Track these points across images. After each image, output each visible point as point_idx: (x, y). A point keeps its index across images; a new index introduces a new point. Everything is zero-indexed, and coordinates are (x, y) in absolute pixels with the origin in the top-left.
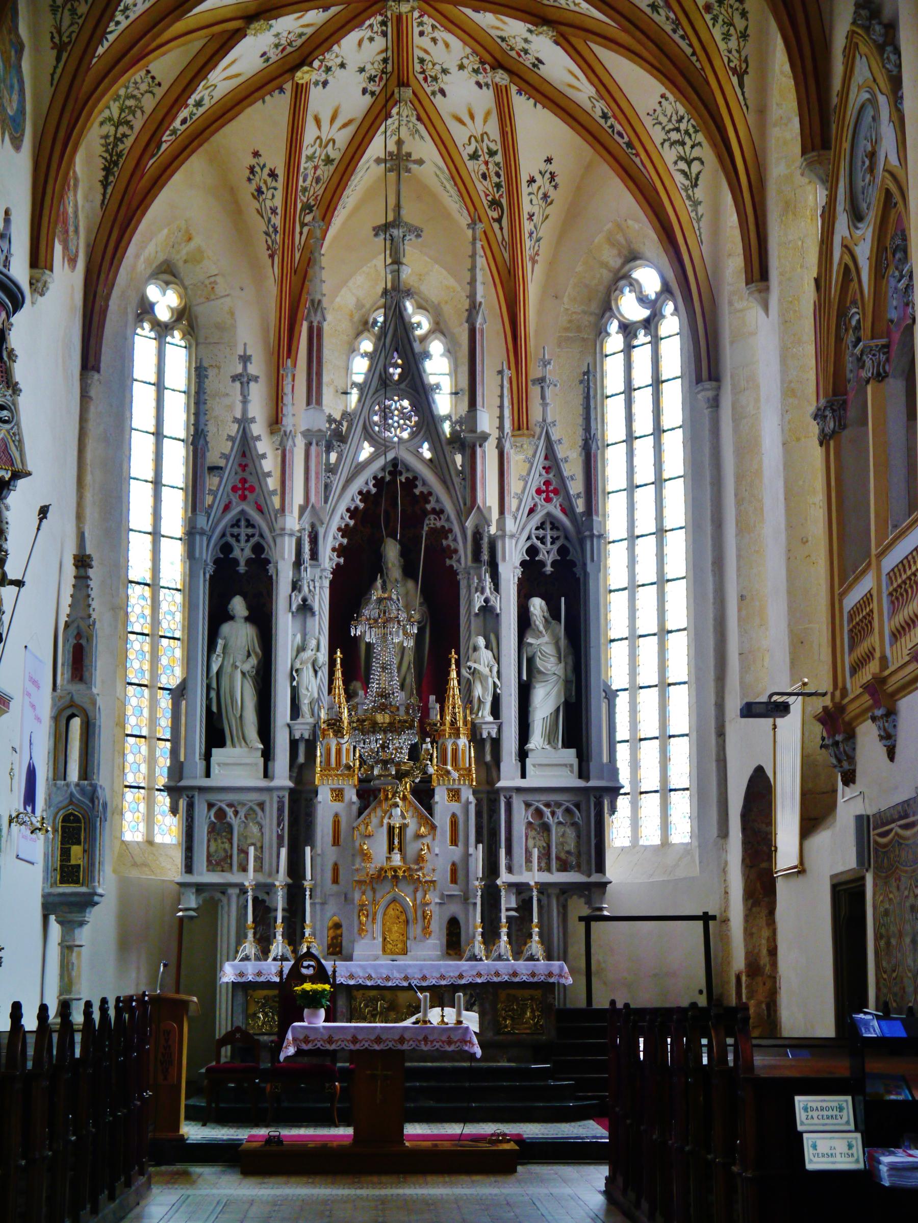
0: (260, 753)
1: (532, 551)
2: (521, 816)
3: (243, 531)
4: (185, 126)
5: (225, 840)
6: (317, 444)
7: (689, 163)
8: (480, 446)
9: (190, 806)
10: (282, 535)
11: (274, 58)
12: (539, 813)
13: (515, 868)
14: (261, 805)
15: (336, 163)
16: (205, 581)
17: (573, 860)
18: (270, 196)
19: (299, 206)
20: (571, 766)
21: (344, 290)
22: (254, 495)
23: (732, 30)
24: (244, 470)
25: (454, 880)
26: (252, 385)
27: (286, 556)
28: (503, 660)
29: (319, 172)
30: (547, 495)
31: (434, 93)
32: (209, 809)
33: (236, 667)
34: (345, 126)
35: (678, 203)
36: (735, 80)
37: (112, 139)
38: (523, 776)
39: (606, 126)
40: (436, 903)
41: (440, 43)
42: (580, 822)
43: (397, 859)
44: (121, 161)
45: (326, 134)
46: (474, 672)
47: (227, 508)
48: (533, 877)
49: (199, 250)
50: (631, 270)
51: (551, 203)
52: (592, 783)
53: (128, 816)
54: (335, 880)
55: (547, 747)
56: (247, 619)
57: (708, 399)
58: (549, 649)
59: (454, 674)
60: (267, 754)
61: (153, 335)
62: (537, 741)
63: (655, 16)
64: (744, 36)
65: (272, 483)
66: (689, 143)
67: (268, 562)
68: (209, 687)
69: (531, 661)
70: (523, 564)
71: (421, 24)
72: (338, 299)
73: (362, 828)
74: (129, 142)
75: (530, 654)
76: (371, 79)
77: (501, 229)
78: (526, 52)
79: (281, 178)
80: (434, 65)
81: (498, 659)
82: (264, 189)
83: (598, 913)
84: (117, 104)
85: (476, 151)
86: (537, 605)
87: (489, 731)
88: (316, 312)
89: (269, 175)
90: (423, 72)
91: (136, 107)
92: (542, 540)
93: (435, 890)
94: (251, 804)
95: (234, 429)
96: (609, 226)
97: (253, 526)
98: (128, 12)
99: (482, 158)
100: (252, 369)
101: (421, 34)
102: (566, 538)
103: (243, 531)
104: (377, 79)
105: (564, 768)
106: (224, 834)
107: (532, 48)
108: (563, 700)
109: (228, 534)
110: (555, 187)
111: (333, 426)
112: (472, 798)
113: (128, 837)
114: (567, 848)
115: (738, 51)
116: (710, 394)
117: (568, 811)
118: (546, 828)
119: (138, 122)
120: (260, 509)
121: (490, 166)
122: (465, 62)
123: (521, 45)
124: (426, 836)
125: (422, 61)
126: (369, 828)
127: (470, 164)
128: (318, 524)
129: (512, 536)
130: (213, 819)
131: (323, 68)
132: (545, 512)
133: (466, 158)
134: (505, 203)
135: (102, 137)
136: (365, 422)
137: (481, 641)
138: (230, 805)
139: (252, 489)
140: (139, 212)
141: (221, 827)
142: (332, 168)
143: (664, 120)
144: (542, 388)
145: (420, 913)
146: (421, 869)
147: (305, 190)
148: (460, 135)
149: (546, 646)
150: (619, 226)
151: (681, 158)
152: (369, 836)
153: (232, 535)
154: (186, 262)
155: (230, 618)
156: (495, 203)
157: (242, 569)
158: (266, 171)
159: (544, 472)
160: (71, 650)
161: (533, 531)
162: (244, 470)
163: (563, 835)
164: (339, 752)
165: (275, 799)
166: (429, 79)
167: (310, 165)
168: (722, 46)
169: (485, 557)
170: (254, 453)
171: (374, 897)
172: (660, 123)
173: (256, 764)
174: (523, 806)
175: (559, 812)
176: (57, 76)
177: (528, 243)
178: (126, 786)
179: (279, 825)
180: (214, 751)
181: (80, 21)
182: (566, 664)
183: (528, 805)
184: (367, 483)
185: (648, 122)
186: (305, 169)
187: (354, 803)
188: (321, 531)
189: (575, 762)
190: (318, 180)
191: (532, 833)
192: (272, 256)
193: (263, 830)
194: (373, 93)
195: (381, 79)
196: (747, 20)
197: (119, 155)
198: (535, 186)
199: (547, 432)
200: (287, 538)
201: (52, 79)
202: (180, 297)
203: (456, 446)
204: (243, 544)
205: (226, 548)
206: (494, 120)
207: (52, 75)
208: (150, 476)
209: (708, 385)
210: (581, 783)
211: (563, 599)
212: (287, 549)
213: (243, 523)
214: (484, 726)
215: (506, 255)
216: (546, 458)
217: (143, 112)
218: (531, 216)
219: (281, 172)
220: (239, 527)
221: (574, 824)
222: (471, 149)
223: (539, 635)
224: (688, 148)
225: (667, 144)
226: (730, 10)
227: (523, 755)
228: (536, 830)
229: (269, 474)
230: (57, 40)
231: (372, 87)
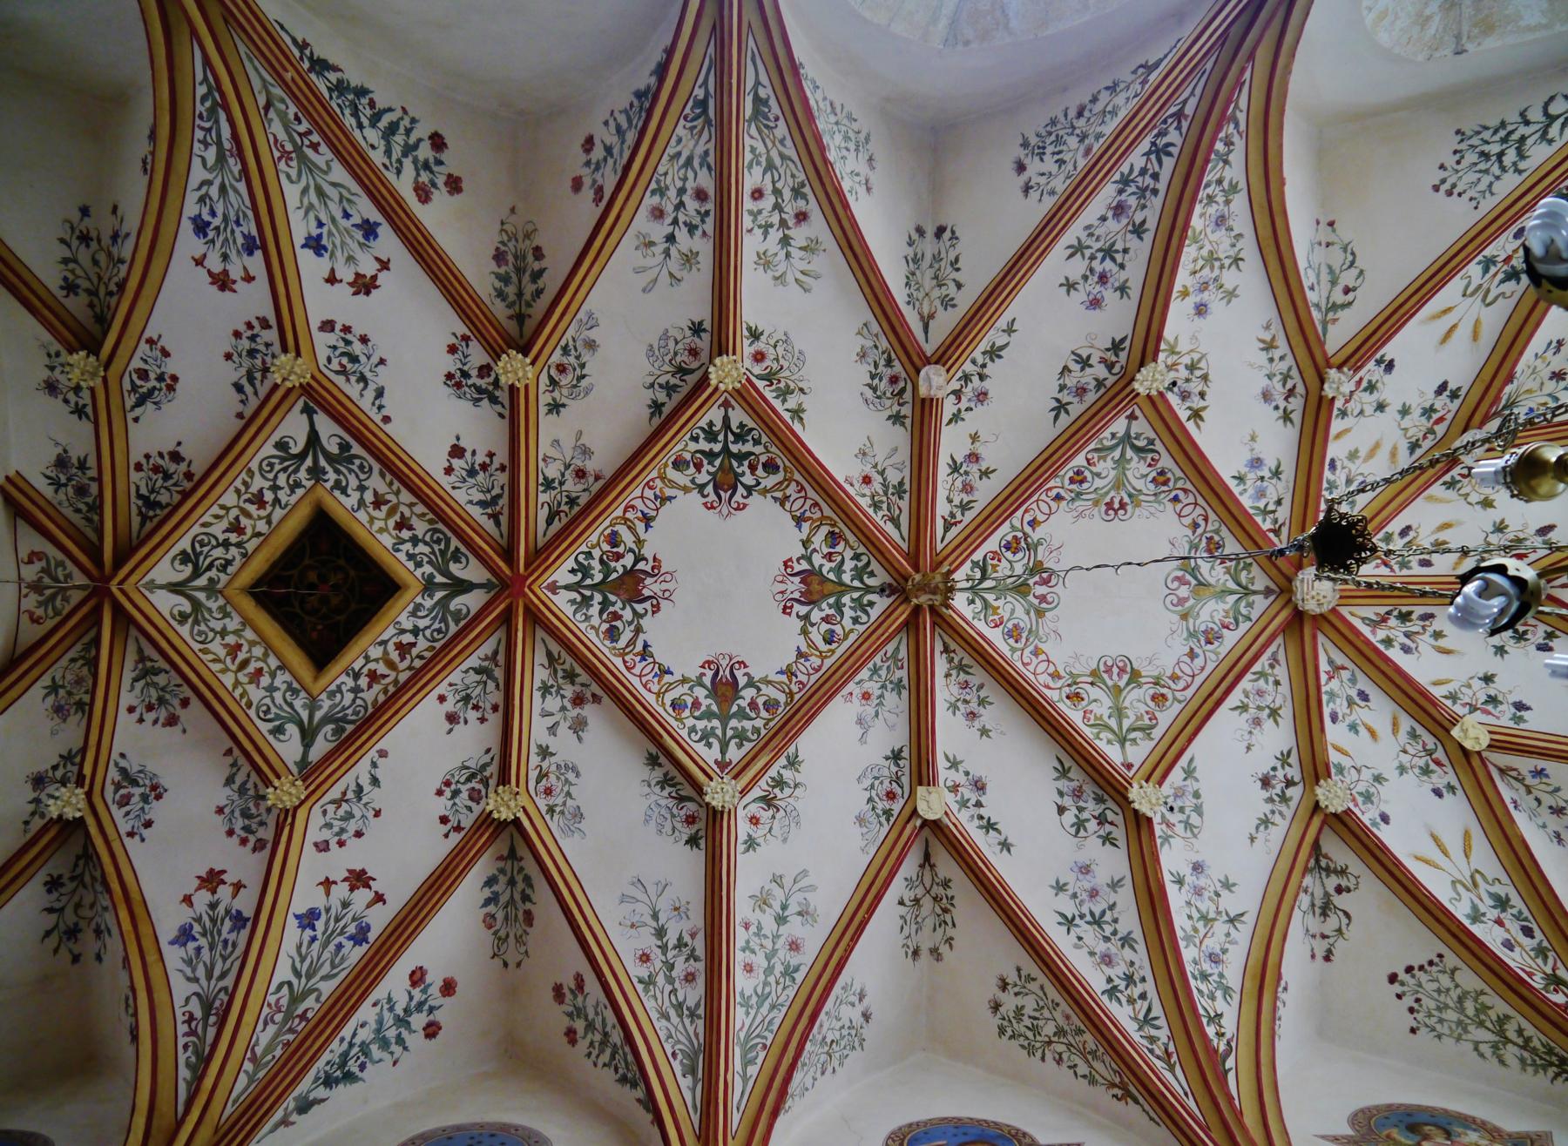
4: (1537, 933)
37: (1526, 1054)
44: (1558, 1050)
63: (1151, 225)
64: (1112, 89)
66: (1523, 130)
74: (1530, 1031)
78: (1428, 411)
91: (1476, 1000)
98: (1136, 977)
107: (1416, 404)
119: (1500, 1007)
122: (1474, 498)
131: (1490, 708)
143: (1486, 179)
185: (1488, 204)
197: (1550, 1051)
217: (1483, 993)
225: (1522, 165)
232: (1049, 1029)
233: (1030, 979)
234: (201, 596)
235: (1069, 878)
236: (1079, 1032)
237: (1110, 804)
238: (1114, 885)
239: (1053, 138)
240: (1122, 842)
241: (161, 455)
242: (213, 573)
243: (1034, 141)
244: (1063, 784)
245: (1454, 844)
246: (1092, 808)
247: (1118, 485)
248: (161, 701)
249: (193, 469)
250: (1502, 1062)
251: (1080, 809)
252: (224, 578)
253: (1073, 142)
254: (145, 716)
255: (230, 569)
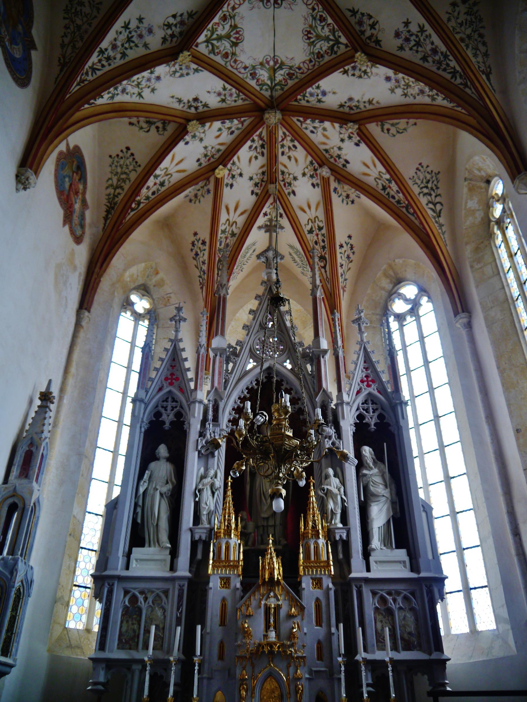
0: (168, 552)
1: (360, 417)
2: (370, 603)
3: (170, 404)
4: (153, 197)
5: (134, 622)
6: (220, 356)
7: (435, 205)
8: (323, 357)
9: (110, 592)
10: (194, 402)
11: (204, 164)
12: (383, 600)
13: (369, 648)
14: (166, 592)
15: (237, 236)
16: (140, 432)
17: (414, 639)
18: (202, 255)
19: (217, 259)
20: (404, 562)
21: (241, 311)
22: (178, 382)
23: (478, 52)
24: (173, 368)
25: (320, 657)
26: (182, 323)
27: (196, 415)
28: (348, 484)
29: (228, 241)
30: (368, 383)
31: (289, 194)
32: (125, 596)
33: (157, 489)
34: (242, 214)
35: (431, 224)
36: (484, 77)
37: (112, 196)
38: (368, 570)
39: (384, 195)
40: (307, 678)
41: (293, 159)
42: (417, 607)
43: (272, 635)
44: (116, 207)
45: (230, 219)
46: (328, 493)
47: (160, 389)
48: (386, 655)
49: (162, 280)
50: (398, 290)
51: (351, 262)
52: (423, 575)
53: (74, 609)
54: (221, 657)
55: (384, 548)
56: (168, 460)
57: (464, 324)
58: (378, 479)
59: (312, 493)
60: (174, 553)
61: (132, 318)
62: (376, 543)
63: (426, 65)
64: (486, 55)
65: (190, 375)
66: (434, 194)
67: (183, 422)
68: (136, 505)
69: (366, 488)
70: (356, 424)
71: (283, 146)
72: (238, 315)
73: (243, 608)
74: (121, 197)
75: (365, 482)
76: (256, 185)
77: (326, 272)
78: (339, 156)
79: (208, 244)
80: (289, 175)
81: (343, 483)
82: (199, 252)
83: (442, 689)
84: (116, 177)
85: (312, 228)
86: (367, 451)
87: (340, 534)
88: (222, 288)
89: (202, 244)
90: (283, 180)
91: (127, 178)
92: (367, 410)
93: (305, 665)
94: (158, 592)
95: (168, 345)
96: (385, 266)
97: (177, 402)
98: (110, 61)
99: (315, 233)
100: (183, 314)
101: (283, 153)
102: (382, 409)
103: (170, 404)
104: (259, 185)
105: (399, 564)
106: (135, 616)
107: (343, 153)
108: (392, 514)
109: (160, 406)
110: (353, 253)
111: (231, 350)
112: (331, 585)
113: (71, 625)
114: (408, 630)
115: (484, 63)
116: (465, 320)
117: (405, 598)
118: (390, 612)
119: (126, 187)
120: (181, 390)
121: (320, 236)
122: (306, 170)
123: (336, 152)
124: (296, 616)
125: (283, 173)
126: (250, 608)
127: (309, 236)
128: (218, 399)
129: (348, 404)
130: (127, 603)
131: (230, 176)
132: (367, 392)
133: (306, 232)
134: (328, 259)
135: (107, 195)
136: (250, 348)
137: (331, 471)
138: (142, 592)
139: (177, 379)
140: (124, 236)
141: (132, 612)
142: (235, 239)
143: (419, 182)
144: (359, 324)
145: (292, 687)
146: (292, 645)
147: (220, 250)
148: (303, 218)
149: (375, 475)
150: (390, 266)
151: (430, 202)
152: (249, 616)
153: (162, 407)
154: (154, 286)
155: (156, 458)
156: (322, 258)
157: (167, 426)
158: (200, 242)
159: (364, 370)
160: (23, 455)
161: (360, 405)
162: (173, 368)
163: (404, 618)
164: (228, 548)
165: (177, 586)
166: (287, 185)
167: (223, 236)
168: (473, 60)
169: (331, 418)
170: (180, 358)
171: (253, 672)
172: (417, 184)
173: (165, 560)
174: (371, 594)
175: (399, 599)
176: (59, 79)
177: (341, 280)
178: (75, 586)
179: (178, 609)
180: (134, 550)
181: (77, 51)
182: (391, 489)
183: (374, 593)
184: (251, 383)
185: (410, 183)
186: (221, 238)
187: (238, 589)
188: (221, 405)
189: (407, 559)
190: (227, 245)
191: (379, 617)
192: (202, 288)
193: (166, 613)
194: (257, 194)
195: (261, 185)
196: (487, 46)
198: (343, 250)
199: (365, 348)
200: (197, 404)
201: (56, 81)
202: (150, 304)
203: (308, 359)
204: (169, 412)
205: (158, 415)
206: (321, 209)
207: (56, 79)
208: (121, 390)
209: (463, 315)
210: (414, 575)
211: (385, 444)
212: (198, 412)
213: (170, 399)
214: (337, 531)
215: (329, 286)
216: (365, 362)
217: (130, 181)
218: (342, 266)
219: (208, 241)
220: (167, 402)
221: (412, 609)
222: (309, 227)
223: (370, 469)
224: (433, 197)
225: (421, 195)
226: (476, 42)
227: (367, 554)
228: (382, 614)
229: (188, 369)
230: (62, 61)
231: (257, 190)
232: (79, 22)
233: (98, 10)
235: (146, 24)
236: (82, 38)
237: (180, 39)
238: (146, 46)
239: (474, 20)
240: (165, 46)
243: (475, 9)
244: (185, 16)
245: (181, 167)
246: (177, 30)
247: (318, 37)
250: (107, 188)
251: (176, 26)
253: (469, 31)
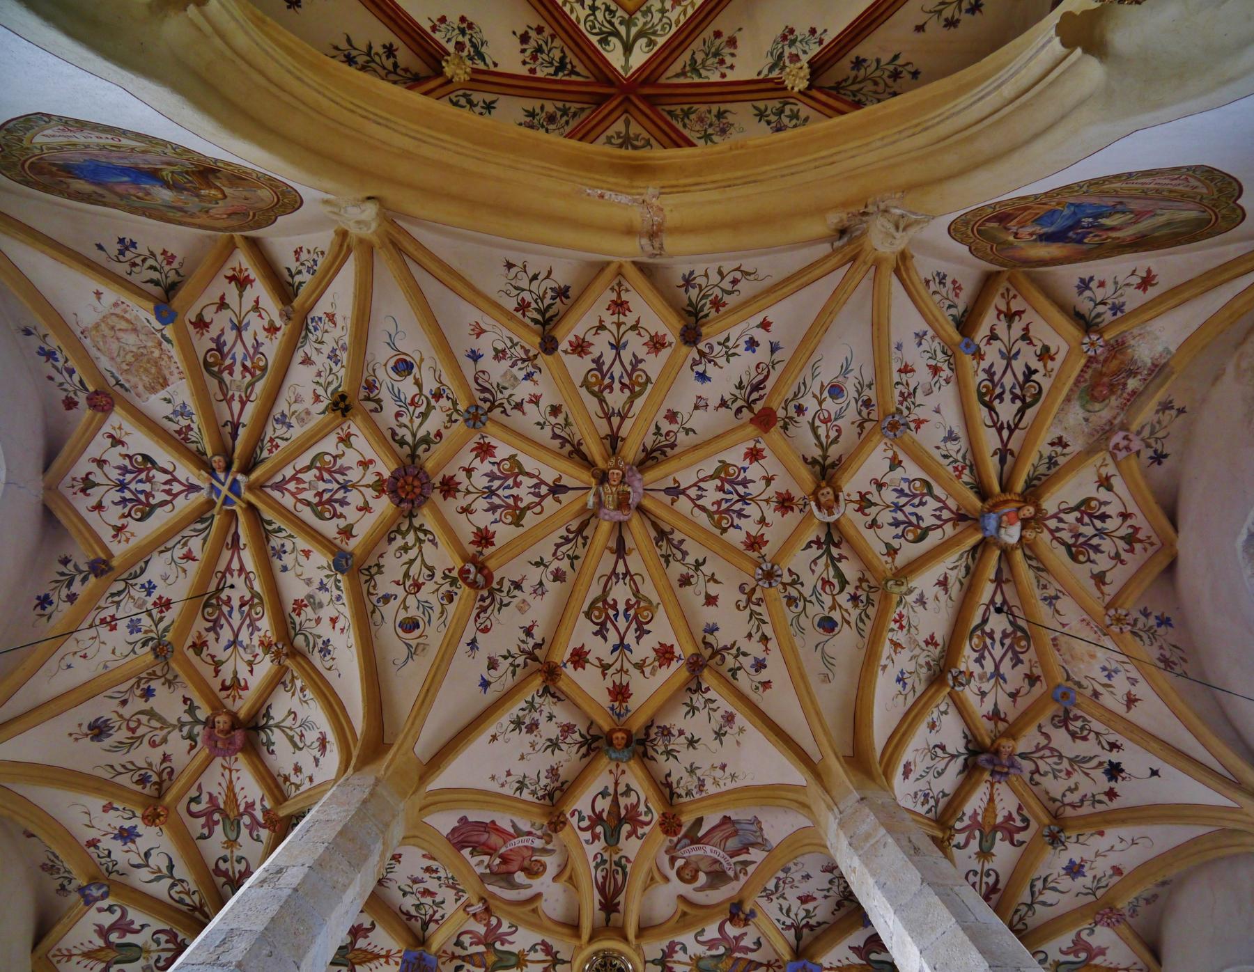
234: (634, 31)
241: (523, 51)
242: (616, 21)
248: (716, 54)
249: (534, 26)
252: (620, 13)
254: (728, 64)
255: (613, 7)
